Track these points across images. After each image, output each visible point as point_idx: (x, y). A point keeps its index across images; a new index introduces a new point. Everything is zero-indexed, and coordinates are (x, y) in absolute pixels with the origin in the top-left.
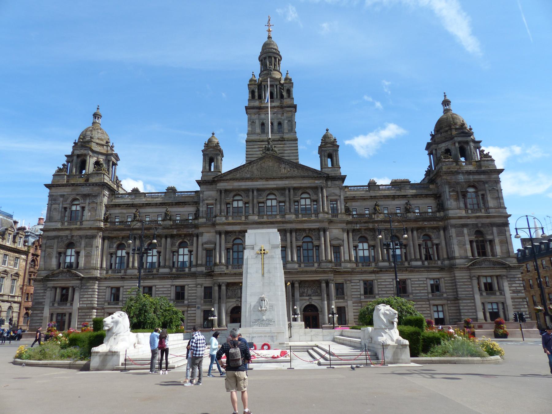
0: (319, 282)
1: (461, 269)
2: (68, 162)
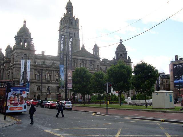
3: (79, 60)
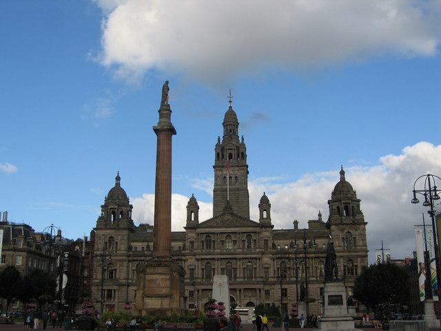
0: (255, 289)
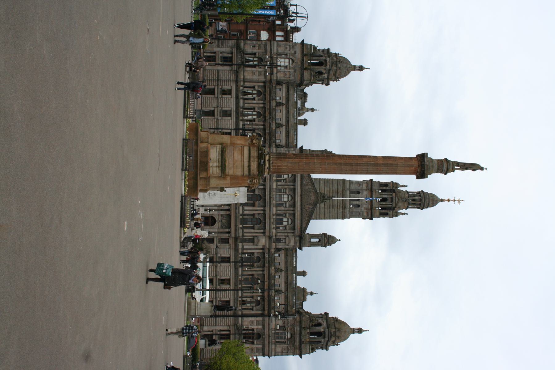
0: (229, 227)
1: (235, 321)
2: (323, 50)
3: (294, 185)
